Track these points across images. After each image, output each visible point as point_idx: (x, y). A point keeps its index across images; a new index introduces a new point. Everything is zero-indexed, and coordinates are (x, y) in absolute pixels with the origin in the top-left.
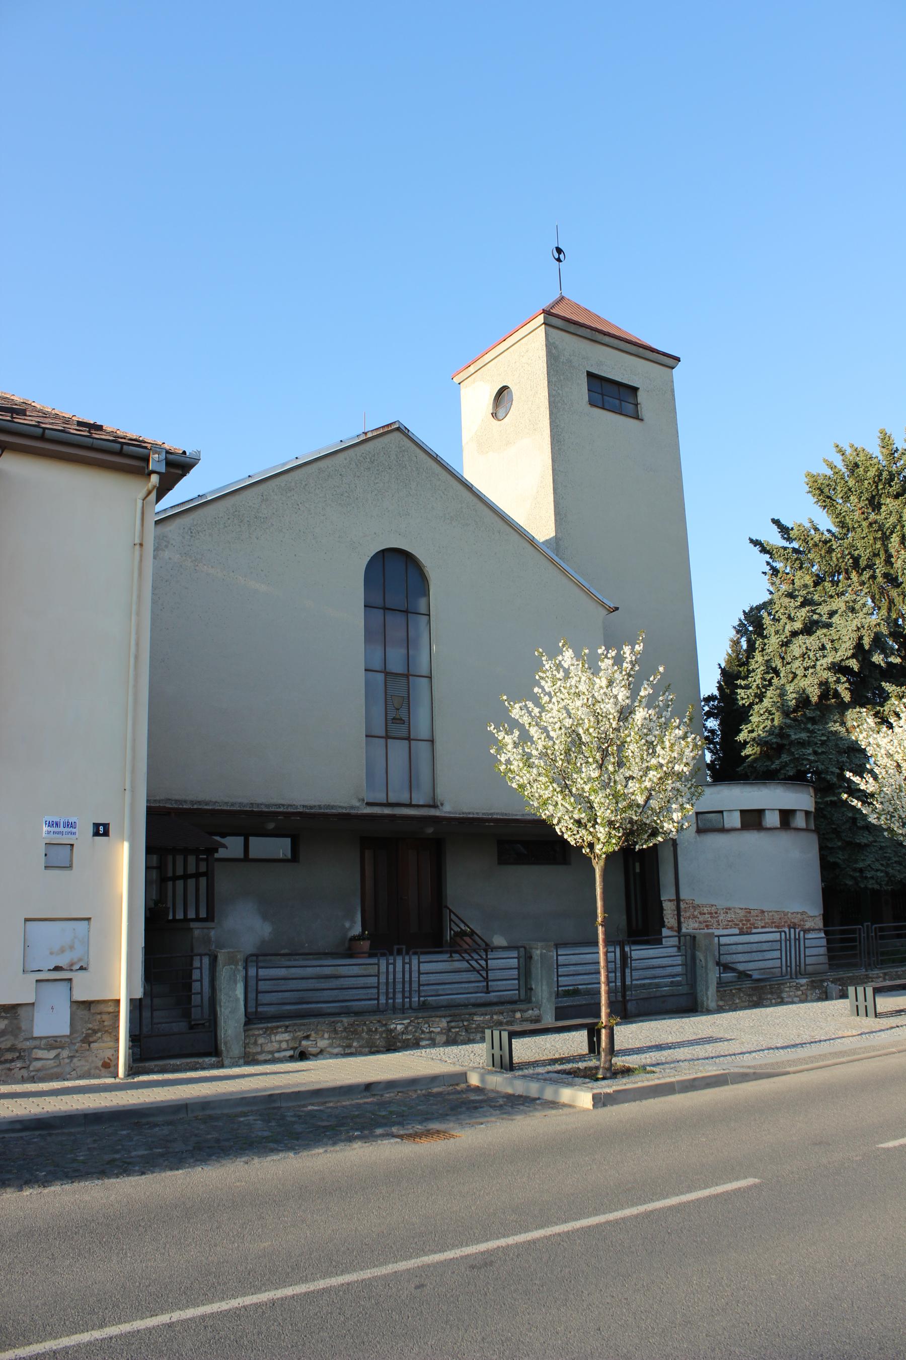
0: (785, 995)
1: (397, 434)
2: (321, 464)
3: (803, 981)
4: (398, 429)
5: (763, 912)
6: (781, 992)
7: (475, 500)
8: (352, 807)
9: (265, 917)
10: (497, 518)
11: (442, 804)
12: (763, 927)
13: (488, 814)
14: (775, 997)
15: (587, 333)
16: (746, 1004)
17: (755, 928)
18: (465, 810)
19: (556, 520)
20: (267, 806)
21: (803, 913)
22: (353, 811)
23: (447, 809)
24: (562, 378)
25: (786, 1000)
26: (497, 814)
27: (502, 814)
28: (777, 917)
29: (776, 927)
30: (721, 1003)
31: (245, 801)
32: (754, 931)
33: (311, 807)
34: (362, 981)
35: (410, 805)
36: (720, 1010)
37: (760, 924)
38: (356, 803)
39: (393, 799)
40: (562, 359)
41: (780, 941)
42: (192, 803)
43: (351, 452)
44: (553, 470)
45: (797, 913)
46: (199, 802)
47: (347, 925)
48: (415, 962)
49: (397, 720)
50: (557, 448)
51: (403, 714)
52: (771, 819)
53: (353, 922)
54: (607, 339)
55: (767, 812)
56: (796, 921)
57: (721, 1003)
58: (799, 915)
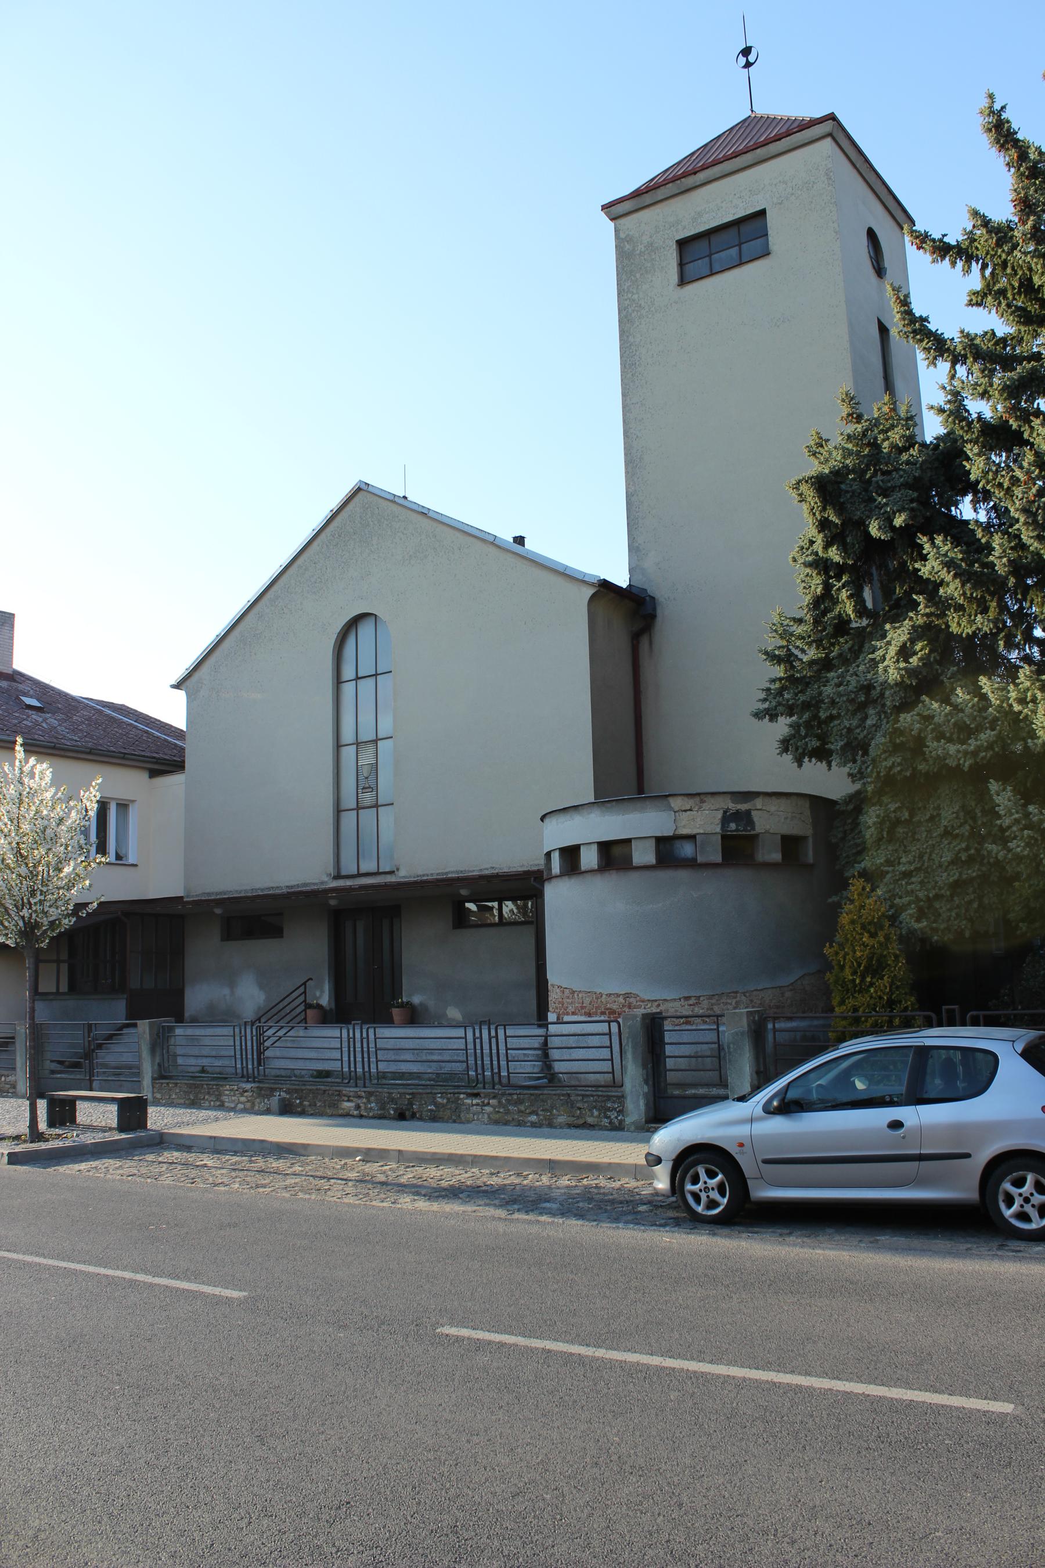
0: (225, 1098)
1: (361, 494)
3: (248, 1086)
4: (359, 489)
5: (573, 992)
6: (220, 1095)
7: (435, 524)
8: (322, 883)
9: (261, 987)
10: (458, 534)
11: (398, 869)
12: (573, 1013)
13: (443, 874)
14: (213, 1098)
15: (671, 189)
16: (182, 1101)
17: (568, 1014)
18: (420, 873)
19: (627, 473)
20: (262, 890)
21: (627, 996)
23: (404, 874)
24: (638, 275)
25: (226, 1104)
26: (452, 872)
27: (457, 872)
28: (587, 1001)
29: (589, 1015)
30: (158, 1096)
31: (248, 888)
32: (566, 1018)
33: (292, 887)
35: (377, 873)
37: (571, 1009)
38: (326, 879)
39: (364, 869)
40: (641, 248)
41: (610, 1034)
42: (217, 894)
43: (323, 535)
44: (624, 407)
45: (618, 995)
46: (221, 893)
47: (318, 994)
48: (371, 1031)
50: (630, 375)
51: (373, 784)
52: (589, 858)
53: (322, 992)
54: (702, 176)
55: (582, 848)
56: (615, 1007)
57: (158, 1096)
58: (621, 999)
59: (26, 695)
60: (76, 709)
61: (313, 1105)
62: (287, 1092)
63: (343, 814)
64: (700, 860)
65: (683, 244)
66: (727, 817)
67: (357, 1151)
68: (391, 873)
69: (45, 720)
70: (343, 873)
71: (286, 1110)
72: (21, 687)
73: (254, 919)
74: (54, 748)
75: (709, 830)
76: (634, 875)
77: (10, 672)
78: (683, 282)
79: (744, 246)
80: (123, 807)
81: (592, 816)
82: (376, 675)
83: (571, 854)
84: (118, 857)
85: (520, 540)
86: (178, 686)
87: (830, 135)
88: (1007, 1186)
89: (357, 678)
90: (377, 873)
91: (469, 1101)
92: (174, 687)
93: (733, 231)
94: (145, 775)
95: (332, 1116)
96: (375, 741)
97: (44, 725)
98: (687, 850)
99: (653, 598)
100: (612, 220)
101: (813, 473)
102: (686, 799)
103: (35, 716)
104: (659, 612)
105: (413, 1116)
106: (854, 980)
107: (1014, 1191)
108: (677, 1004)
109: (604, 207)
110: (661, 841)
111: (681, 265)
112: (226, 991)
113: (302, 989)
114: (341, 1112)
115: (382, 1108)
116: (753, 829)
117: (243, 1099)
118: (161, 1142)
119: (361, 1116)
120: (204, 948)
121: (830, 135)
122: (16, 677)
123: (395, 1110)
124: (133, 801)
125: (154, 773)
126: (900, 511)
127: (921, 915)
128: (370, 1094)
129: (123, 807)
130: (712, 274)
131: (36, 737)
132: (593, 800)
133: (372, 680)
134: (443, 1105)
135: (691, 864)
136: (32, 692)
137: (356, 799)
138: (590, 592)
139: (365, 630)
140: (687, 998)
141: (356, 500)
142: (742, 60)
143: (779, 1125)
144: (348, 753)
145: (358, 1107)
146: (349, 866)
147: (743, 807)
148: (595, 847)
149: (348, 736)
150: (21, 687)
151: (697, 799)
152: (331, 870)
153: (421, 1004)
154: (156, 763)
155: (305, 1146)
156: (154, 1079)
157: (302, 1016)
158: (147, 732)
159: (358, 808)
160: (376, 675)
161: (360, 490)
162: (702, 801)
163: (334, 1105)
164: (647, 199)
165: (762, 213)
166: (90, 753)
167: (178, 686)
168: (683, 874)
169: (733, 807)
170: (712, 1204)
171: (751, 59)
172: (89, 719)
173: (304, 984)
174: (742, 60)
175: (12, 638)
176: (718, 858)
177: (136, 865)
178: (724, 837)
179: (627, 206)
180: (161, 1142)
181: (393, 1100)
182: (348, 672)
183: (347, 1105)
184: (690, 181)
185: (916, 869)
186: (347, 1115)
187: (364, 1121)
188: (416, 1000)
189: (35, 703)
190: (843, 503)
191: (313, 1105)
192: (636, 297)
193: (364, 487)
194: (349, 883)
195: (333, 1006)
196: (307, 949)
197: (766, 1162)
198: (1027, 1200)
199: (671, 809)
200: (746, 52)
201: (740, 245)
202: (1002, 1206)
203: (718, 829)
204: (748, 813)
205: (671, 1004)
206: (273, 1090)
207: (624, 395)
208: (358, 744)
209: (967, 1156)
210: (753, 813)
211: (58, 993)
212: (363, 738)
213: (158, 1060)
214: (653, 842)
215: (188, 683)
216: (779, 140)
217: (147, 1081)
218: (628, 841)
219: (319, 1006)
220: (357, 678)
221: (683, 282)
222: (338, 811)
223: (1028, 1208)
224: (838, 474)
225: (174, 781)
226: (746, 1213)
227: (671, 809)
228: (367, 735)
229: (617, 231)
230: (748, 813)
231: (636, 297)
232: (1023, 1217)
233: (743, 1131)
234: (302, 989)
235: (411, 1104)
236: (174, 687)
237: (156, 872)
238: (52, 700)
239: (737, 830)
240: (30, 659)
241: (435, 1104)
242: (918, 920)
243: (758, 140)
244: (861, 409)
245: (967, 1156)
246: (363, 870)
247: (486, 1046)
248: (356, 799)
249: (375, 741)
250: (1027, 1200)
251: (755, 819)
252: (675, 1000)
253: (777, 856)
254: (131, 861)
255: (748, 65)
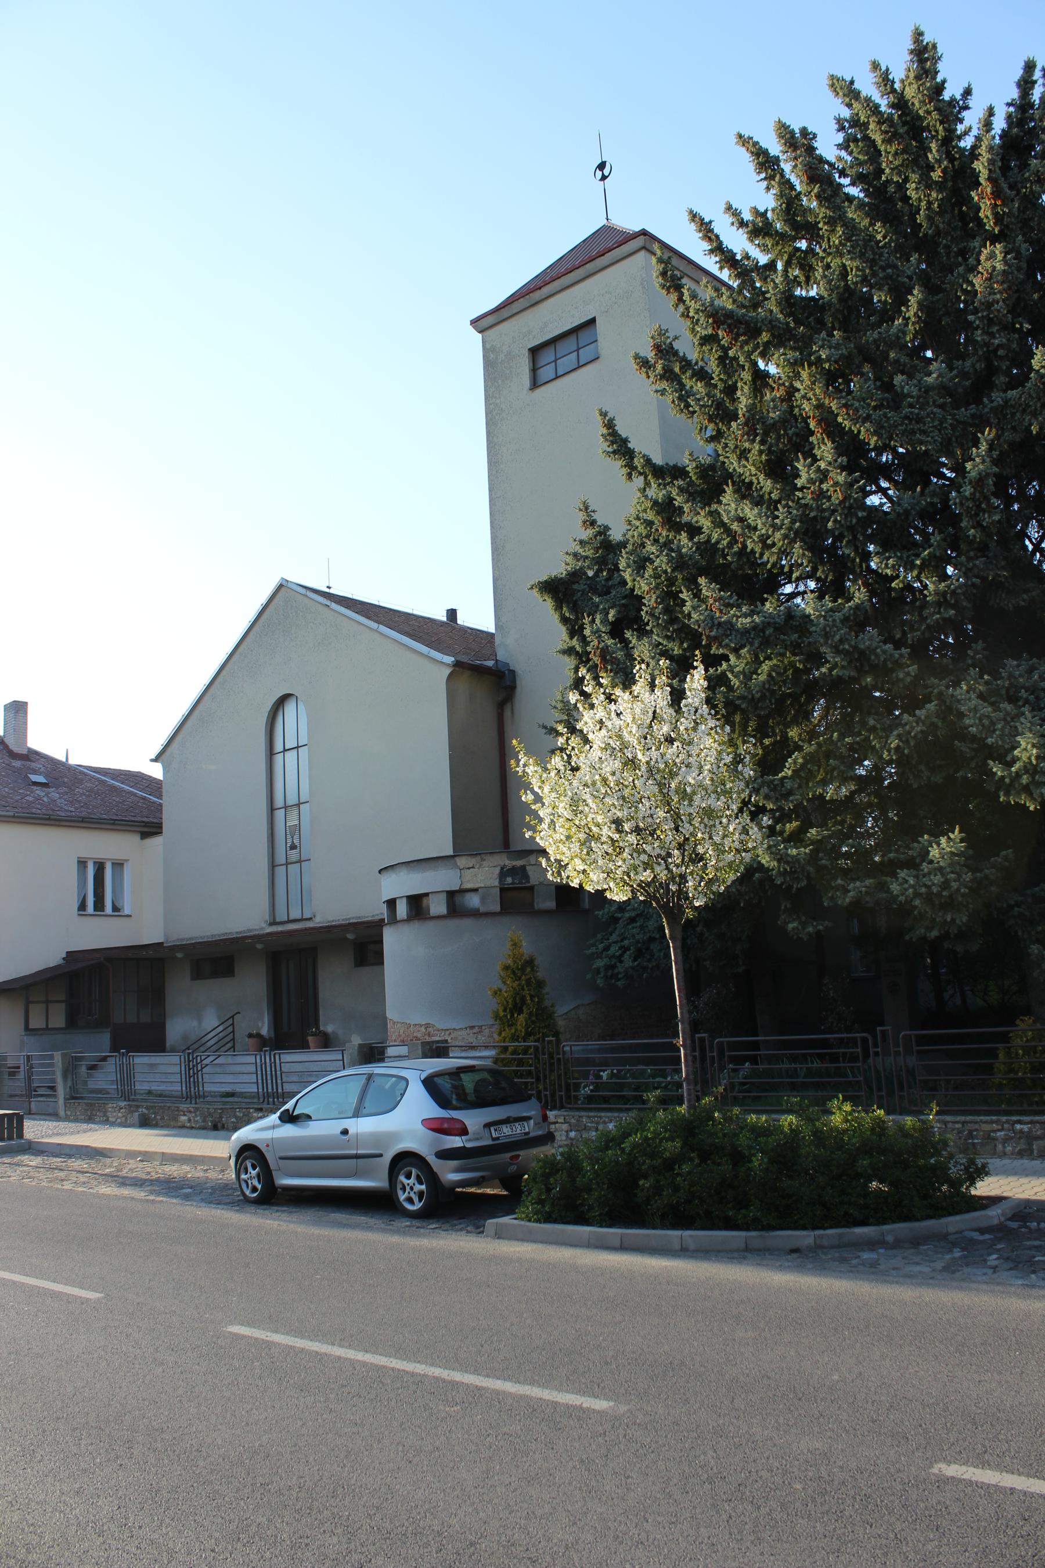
1: (283, 590)
2: (240, 650)
3: (123, 1104)
8: (262, 929)
14: (102, 1114)
19: (493, 559)
21: (427, 1026)
22: (262, 932)
23: (319, 921)
27: (357, 918)
30: (69, 1113)
33: (240, 932)
34: (243, 1069)
35: (302, 920)
36: (67, 1119)
40: (502, 356)
45: (421, 1026)
49: (293, 847)
53: (263, 1023)
54: (546, 291)
58: (423, 1029)
59: (35, 772)
60: (81, 782)
61: (162, 1118)
62: (147, 1108)
63: (277, 869)
64: (482, 910)
65: (535, 351)
66: (504, 873)
67: (140, 1153)
68: (310, 919)
69: (47, 795)
70: (278, 920)
71: (145, 1123)
72: (33, 765)
73: (215, 959)
74: (49, 819)
75: (488, 884)
76: (430, 925)
77: (25, 752)
78: (535, 385)
79: (581, 351)
80: (118, 865)
81: (402, 874)
82: (298, 747)
83: (416, 903)
84: (115, 909)
85: (452, 614)
86: (156, 760)
87: (644, 248)
88: (402, 1178)
89: (285, 750)
90: (302, 920)
91: (255, 1115)
92: (152, 760)
93: (572, 339)
94: (137, 838)
95: (174, 1127)
96: (298, 805)
97: (45, 799)
98: (474, 901)
99: (513, 673)
100: (480, 332)
101: (544, 578)
102: (469, 858)
103: (39, 791)
104: (518, 683)
105: (223, 1127)
106: (506, 1016)
107: (406, 1181)
108: (464, 1032)
109: (474, 322)
110: (451, 895)
111: (534, 370)
112: (195, 1023)
113: (230, 1021)
114: (179, 1124)
115: (204, 1121)
116: (528, 882)
117: (120, 1115)
118: (32, 1148)
119: (192, 1128)
120: (180, 987)
121: (644, 248)
122: (32, 756)
123: (212, 1122)
124: (127, 860)
125: (145, 835)
126: (612, 608)
127: (638, 954)
128: (197, 1109)
129: (118, 865)
130: (557, 377)
131: (34, 811)
132: (451, 853)
133: (295, 752)
134: (241, 1118)
135: (475, 914)
136: (43, 769)
137: (282, 854)
138: (447, 671)
139: (290, 708)
140: (472, 1027)
141: (280, 594)
142: (599, 174)
143: (290, 1131)
144: (280, 814)
145: (189, 1120)
146: (281, 916)
147: (518, 863)
148: (405, 900)
149: (279, 802)
150: (33, 765)
151: (478, 858)
152: (267, 917)
153: (333, 1032)
154: (145, 826)
155: (111, 1150)
156: (65, 1099)
157: (230, 1045)
158: (144, 798)
159: (287, 864)
160: (298, 747)
161: (280, 587)
162: (483, 860)
163: (175, 1119)
164: (505, 313)
165: (592, 321)
166: (82, 821)
167: (156, 760)
168: (467, 923)
169: (509, 863)
170: (254, 1190)
171: (606, 172)
172: (91, 790)
173: (233, 1017)
174: (599, 174)
175: (26, 723)
176: (496, 907)
177: (130, 916)
178: (502, 890)
179: (490, 320)
180: (32, 1148)
181: (210, 1114)
182: (279, 747)
183: (183, 1118)
184: (537, 295)
185: (637, 915)
186: (183, 1127)
187: (194, 1131)
188: (330, 1029)
189: (41, 779)
190: (576, 601)
191: (162, 1118)
192: (498, 401)
193: (285, 583)
194: (280, 928)
195: (273, 1036)
196: (251, 986)
197: (281, 1158)
198: (412, 1188)
199: (457, 867)
200: (602, 166)
201: (578, 350)
202: (400, 1192)
203: (497, 883)
204: (523, 868)
205: (459, 1033)
206: (138, 1107)
207: (490, 490)
208: (286, 807)
209: (381, 1155)
210: (528, 868)
211: (47, 1028)
212: (290, 802)
213: (69, 1083)
214: (444, 895)
215: (164, 757)
216: (603, 255)
217: (61, 1101)
218: (427, 895)
219: (258, 1036)
220: (285, 750)
221: (535, 385)
222: (273, 866)
223: (412, 1195)
224: (575, 575)
225: (156, 841)
226: (272, 1197)
227: (457, 867)
228: (292, 800)
229: (484, 342)
230: (523, 868)
231: (498, 401)
232: (410, 1200)
233: (268, 1135)
234: (230, 1021)
235: (221, 1117)
236: (152, 760)
237: (145, 918)
238: (60, 774)
239: (513, 883)
240: (44, 738)
241: (236, 1117)
242: (635, 960)
243: (605, 247)
244: (595, 516)
245: (381, 1155)
246: (292, 917)
247: (268, 1069)
248: (282, 854)
249: (298, 805)
250: (412, 1188)
251: (530, 873)
252: (461, 1029)
253: (551, 904)
254: (126, 912)
255: (604, 178)
